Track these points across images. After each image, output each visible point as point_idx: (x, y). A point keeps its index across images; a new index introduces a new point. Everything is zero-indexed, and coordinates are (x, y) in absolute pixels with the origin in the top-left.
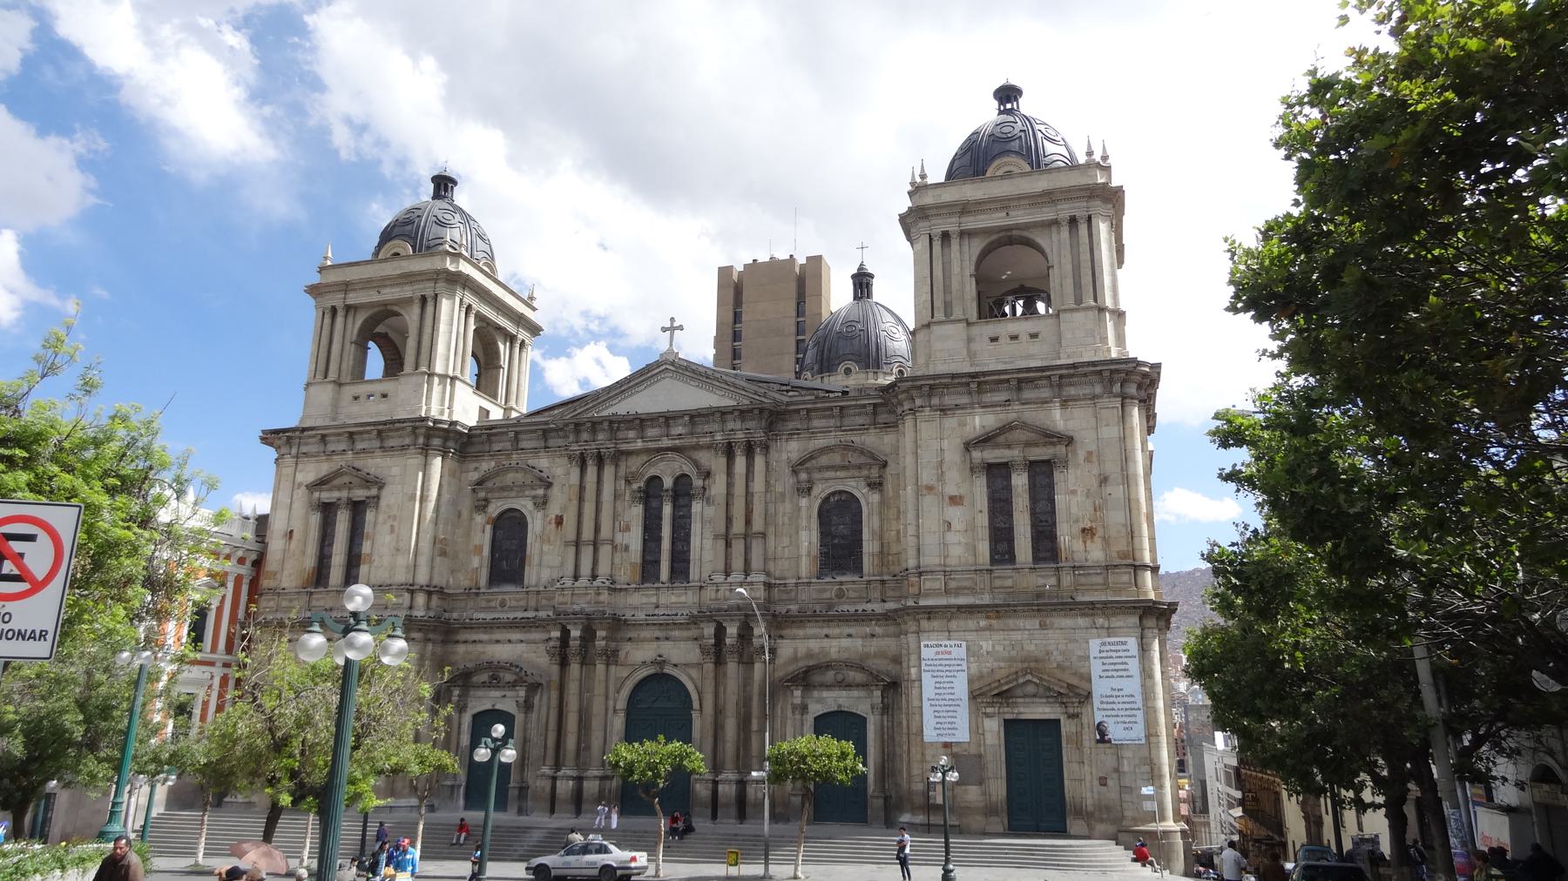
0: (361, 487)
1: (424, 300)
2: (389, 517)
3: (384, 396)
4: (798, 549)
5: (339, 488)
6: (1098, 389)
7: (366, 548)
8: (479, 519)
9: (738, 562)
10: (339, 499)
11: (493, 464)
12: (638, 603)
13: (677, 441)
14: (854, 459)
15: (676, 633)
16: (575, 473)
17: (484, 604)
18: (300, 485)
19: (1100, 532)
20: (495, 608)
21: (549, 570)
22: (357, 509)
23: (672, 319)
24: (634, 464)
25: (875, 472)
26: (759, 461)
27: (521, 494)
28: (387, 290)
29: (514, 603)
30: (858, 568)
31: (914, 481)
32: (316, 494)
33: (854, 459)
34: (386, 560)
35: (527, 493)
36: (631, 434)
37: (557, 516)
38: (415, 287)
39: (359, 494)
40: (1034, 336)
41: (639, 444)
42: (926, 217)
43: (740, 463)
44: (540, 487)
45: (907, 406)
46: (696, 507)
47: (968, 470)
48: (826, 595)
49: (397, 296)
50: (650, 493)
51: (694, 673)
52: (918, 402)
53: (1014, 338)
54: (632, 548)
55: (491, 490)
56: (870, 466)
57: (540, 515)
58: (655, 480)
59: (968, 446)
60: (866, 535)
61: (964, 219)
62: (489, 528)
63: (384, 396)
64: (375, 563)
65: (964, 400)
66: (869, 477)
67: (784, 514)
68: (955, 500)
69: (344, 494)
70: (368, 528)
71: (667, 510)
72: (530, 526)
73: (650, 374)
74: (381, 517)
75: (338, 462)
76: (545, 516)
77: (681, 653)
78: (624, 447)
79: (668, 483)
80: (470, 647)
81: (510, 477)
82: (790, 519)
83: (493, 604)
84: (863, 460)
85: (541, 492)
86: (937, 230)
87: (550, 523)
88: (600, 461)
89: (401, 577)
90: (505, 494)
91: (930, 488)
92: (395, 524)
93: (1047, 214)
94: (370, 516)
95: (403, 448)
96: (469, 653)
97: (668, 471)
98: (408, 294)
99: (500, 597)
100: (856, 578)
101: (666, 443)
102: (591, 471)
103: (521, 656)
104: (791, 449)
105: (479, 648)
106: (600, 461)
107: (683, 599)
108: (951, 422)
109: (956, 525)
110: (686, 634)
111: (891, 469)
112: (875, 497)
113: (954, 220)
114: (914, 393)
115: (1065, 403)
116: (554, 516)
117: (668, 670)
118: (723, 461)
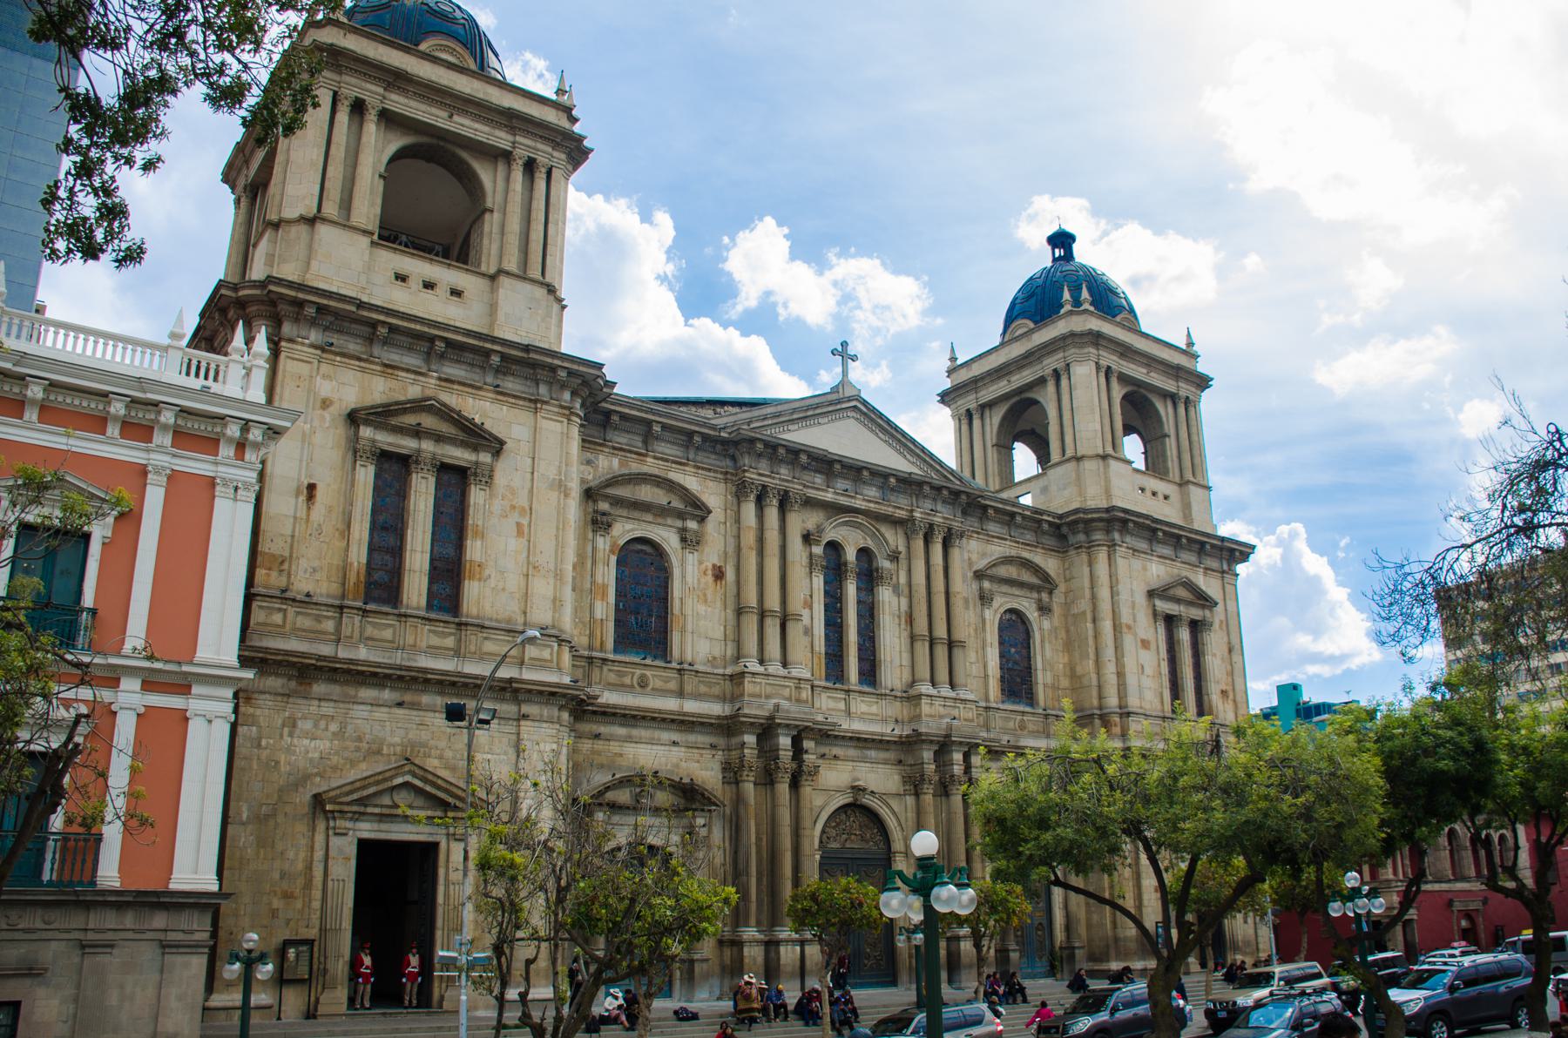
0: (464, 444)
1: (530, 166)
2: (513, 507)
3: (456, 293)
4: (985, 667)
5: (417, 433)
6: (1225, 567)
7: (474, 550)
8: (602, 543)
9: (942, 674)
10: (419, 451)
11: (616, 462)
12: (828, 707)
13: (872, 505)
14: (1027, 577)
15: (872, 753)
16: (749, 510)
17: (612, 678)
18: (325, 404)
19: (1231, 697)
20: (632, 686)
21: (708, 642)
22: (455, 480)
23: (844, 344)
24: (812, 519)
25: (1045, 596)
26: (955, 553)
27: (660, 520)
28: (466, 122)
29: (659, 684)
30: (1031, 699)
31: (1110, 616)
32: (366, 432)
33: (1027, 577)
34: (514, 582)
35: (669, 521)
36: (819, 480)
37: (714, 566)
38: (518, 138)
39: (460, 455)
40: (1166, 498)
41: (829, 496)
42: (1097, 345)
43: (937, 549)
44: (694, 517)
45: (1098, 536)
46: (885, 595)
47: (1151, 617)
48: (1011, 724)
49: (481, 138)
50: (833, 564)
51: (894, 804)
52: (1117, 536)
53: (1154, 494)
54: (816, 632)
55: (618, 502)
56: (1038, 589)
57: (691, 558)
58: (834, 547)
59: (1151, 594)
60: (1038, 662)
61: (1121, 362)
62: (614, 559)
63: (456, 293)
64: (492, 582)
65: (1143, 545)
66: (1040, 600)
67: (969, 625)
68: (1145, 644)
69: (427, 446)
70: (474, 518)
71: (851, 589)
72: (676, 572)
73: (839, 407)
74: (497, 505)
75: (413, 390)
76: (700, 563)
77: (880, 778)
78: (812, 493)
79: (851, 555)
80: (599, 745)
81: (646, 493)
82: (976, 630)
83: (627, 680)
84: (1034, 580)
85: (692, 525)
86: (1103, 363)
87: (705, 573)
88: (784, 504)
89: (541, 614)
90: (636, 514)
91: (1129, 627)
92: (525, 522)
93: (1169, 385)
94: (476, 496)
95: (535, 403)
96: (599, 753)
97: (852, 542)
98: (505, 145)
99: (638, 672)
100: (1028, 709)
101: (859, 503)
102: (772, 514)
103: (677, 766)
104: (975, 551)
105: (614, 747)
106: (784, 504)
107: (874, 709)
108: (1137, 563)
109: (1149, 670)
110: (883, 755)
111: (1058, 598)
112: (1046, 624)
113: (1115, 358)
114: (1117, 525)
115: (1205, 574)
116: (710, 566)
117: (867, 800)
118: (919, 544)
